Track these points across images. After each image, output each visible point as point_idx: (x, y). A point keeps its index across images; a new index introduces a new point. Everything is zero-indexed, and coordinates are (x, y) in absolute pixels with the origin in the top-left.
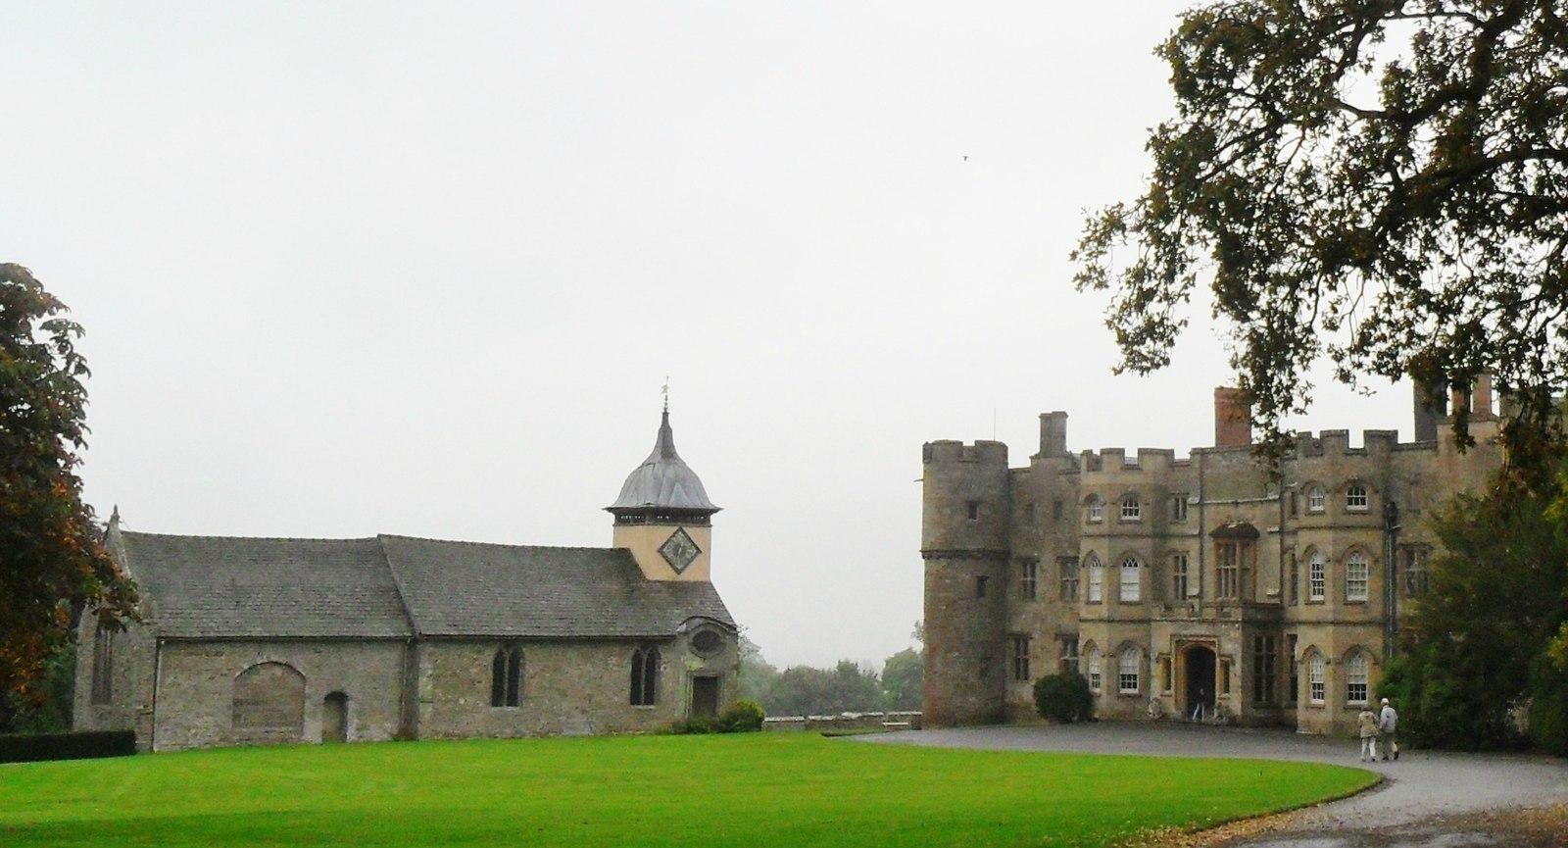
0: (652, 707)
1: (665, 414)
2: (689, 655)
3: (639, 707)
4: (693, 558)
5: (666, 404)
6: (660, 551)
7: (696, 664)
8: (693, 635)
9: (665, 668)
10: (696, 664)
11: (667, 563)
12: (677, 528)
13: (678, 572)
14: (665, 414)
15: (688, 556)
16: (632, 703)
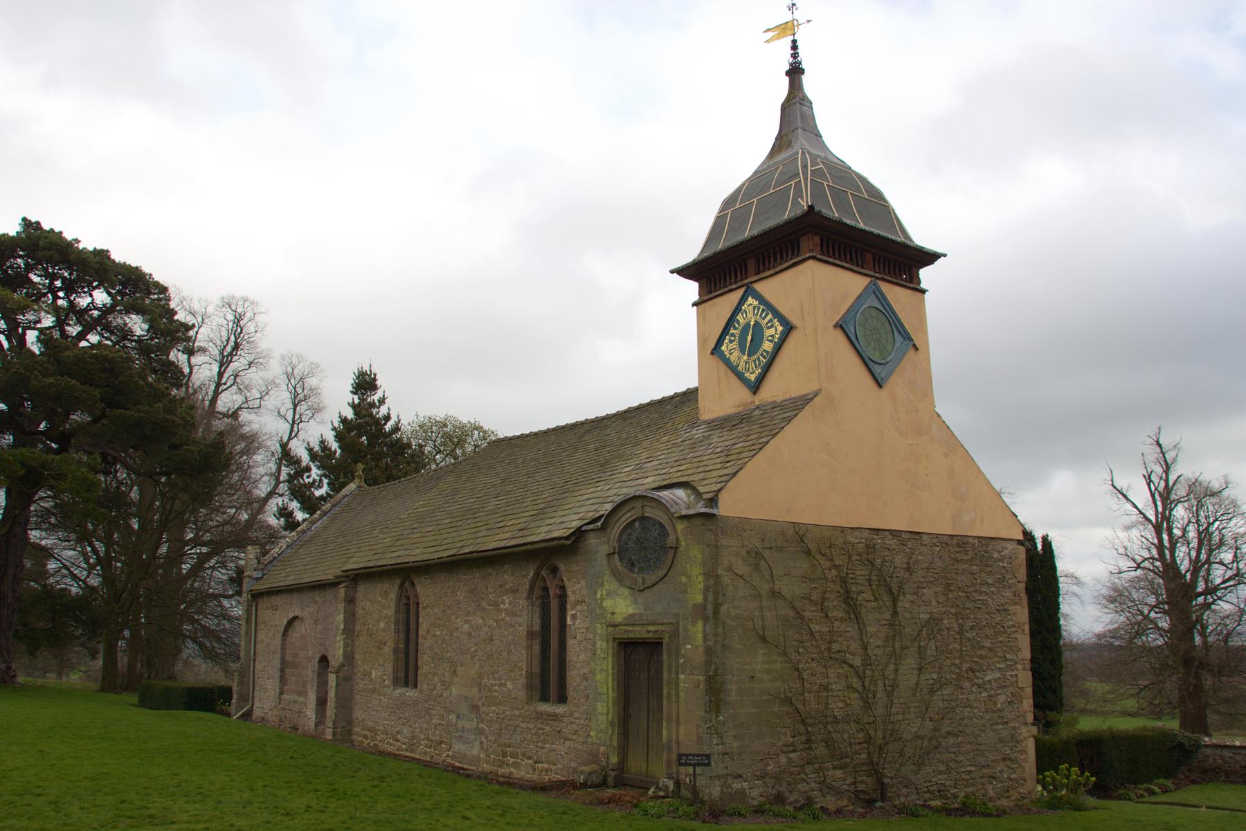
0: (560, 709)
1: (795, 72)
2: (610, 584)
3: (546, 707)
4: (778, 348)
5: (795, 56)
6: (716, 350)
7: (622, 605)
8: (615, 531)
9: (574, 617)
10: (622, 605)
11: (734, 378)
12: (740, 292)
13: (755, 387)
14: (795, 72)
15: (768, 346)
16: (545, 698)
